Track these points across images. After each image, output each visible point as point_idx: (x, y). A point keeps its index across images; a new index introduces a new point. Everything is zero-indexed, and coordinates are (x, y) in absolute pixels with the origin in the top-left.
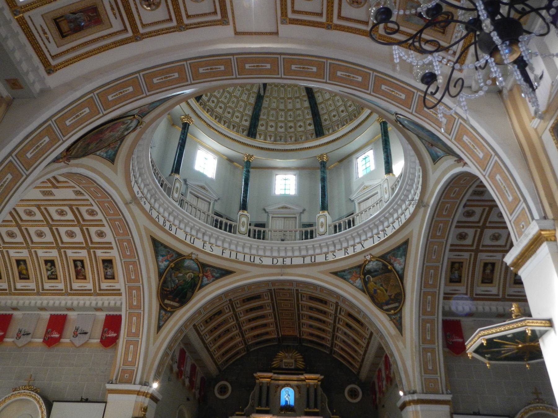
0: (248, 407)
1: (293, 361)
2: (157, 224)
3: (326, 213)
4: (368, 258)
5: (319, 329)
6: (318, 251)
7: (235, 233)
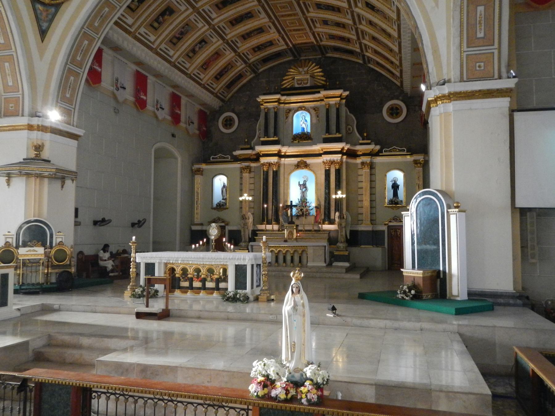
1: (308, 76)
5: (338, 25)
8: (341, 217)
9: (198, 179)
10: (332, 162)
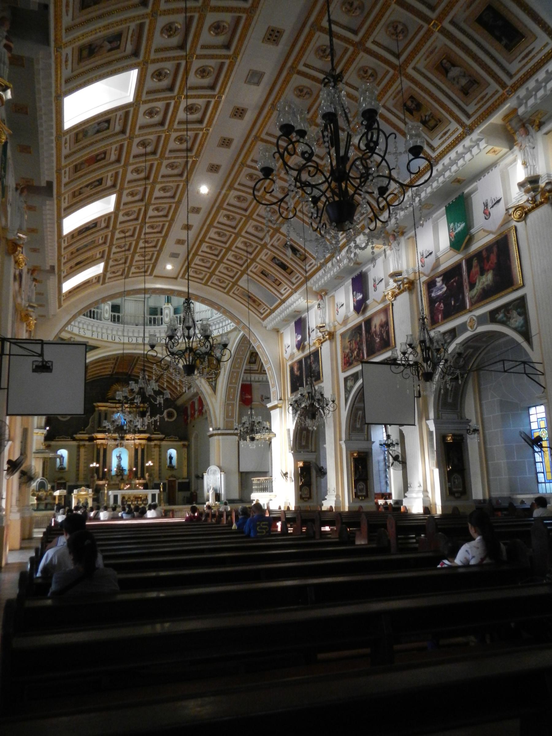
0: (89, 427)
3: (170, 305)
7: (101, 320)
8: (150, 475)
10: (140, 444)
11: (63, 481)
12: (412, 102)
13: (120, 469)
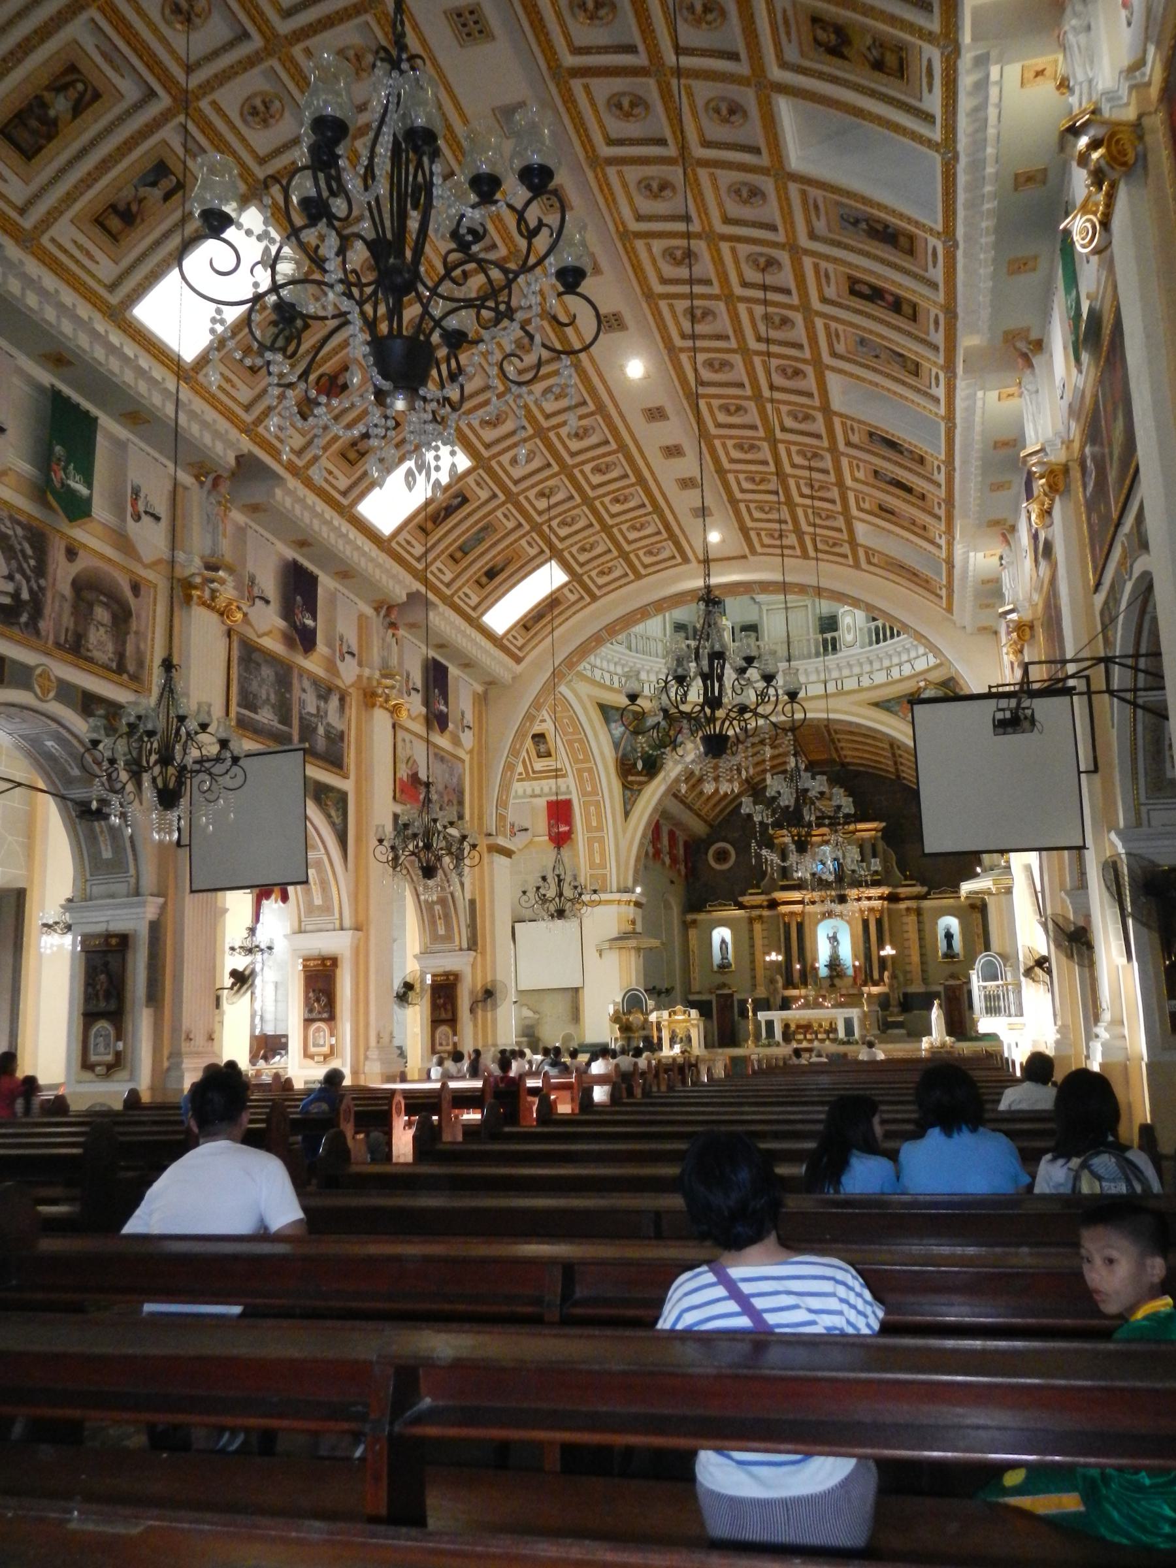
2: (603, 686)
4: (922, 684)
6: (846, 672)
8: (893, 976)
9: (693, 933)
10: (871, 910)
11: (726, 991)
12: (824, 29)
13: (834, 964)
